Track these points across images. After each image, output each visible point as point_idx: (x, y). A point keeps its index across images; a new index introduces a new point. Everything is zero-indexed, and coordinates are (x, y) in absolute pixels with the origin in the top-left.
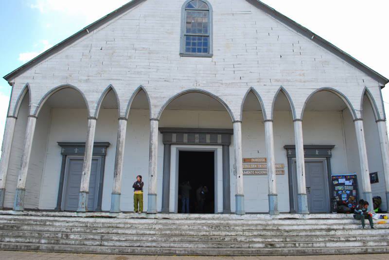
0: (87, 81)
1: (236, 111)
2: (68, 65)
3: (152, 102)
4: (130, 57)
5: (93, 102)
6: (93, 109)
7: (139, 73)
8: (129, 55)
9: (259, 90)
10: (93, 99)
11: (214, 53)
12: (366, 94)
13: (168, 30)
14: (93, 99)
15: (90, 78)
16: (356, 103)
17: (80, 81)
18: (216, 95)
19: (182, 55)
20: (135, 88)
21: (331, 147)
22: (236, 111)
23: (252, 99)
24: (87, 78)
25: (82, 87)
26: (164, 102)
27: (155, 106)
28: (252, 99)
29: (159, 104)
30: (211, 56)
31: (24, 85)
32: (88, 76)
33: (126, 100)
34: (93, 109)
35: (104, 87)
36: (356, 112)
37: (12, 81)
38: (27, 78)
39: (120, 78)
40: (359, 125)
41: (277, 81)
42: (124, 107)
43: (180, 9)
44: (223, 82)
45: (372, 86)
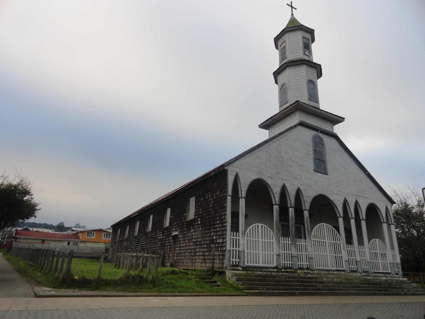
0: (271, 178)
2: (260, 164)
3: (305, 198)
4: (291, 166)
5: (276, 193)
7: (296, 178)
8: (290, 164)
9: (349, 200)
11: (329, 173)
13: (307, 152)
14: (276, 191)
15: (273, 176)
17: (268, 177)
18: (332, 199)
20: (296, 188)
23: (345, 203)
24: (270, 176)
25: (270, 182)
27: (307, 202)
29: (308, 200)
30: (326, 174)
31: (235, 173)
32: (271, 175)
33: (292, 195)
35: (281, 185)
36: (384, 218)
37: (226, 168)
38: (236, 167)
39: (288, 179)
40: (385, 226)
41: (354, 195)
43: (311, 140)
44: (334, 192)
45: (389, 204)
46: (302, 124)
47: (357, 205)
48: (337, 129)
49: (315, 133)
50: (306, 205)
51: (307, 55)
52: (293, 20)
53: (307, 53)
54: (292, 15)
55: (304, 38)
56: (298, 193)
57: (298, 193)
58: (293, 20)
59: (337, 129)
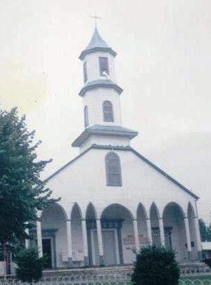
1: (134, 214)
6: (69, 216)
10: (68, 210)
12: (190, 205)
14: (68, 210)
16: (185, 209)
19: (108, 185)
20: (88, 204)
21: (171, 228)
22: (134, 214)
26: (102, 210)
28: (141, 208)
34: (69, 216)
40: (186, 221)
42: (84, 216)
45: (192, 200)
46: (94, 147)
47: (154, 209)
48: (133, 143)
49: (106, 152)
50: (99, 214)
51: (104, 75)
52: (96, 36)
53: (104, 73)
54: (96, 29)
55: (100, 58)
56: (91, 208)
57: (91, 208)
58: (96, 36)
59: (133, 143)
